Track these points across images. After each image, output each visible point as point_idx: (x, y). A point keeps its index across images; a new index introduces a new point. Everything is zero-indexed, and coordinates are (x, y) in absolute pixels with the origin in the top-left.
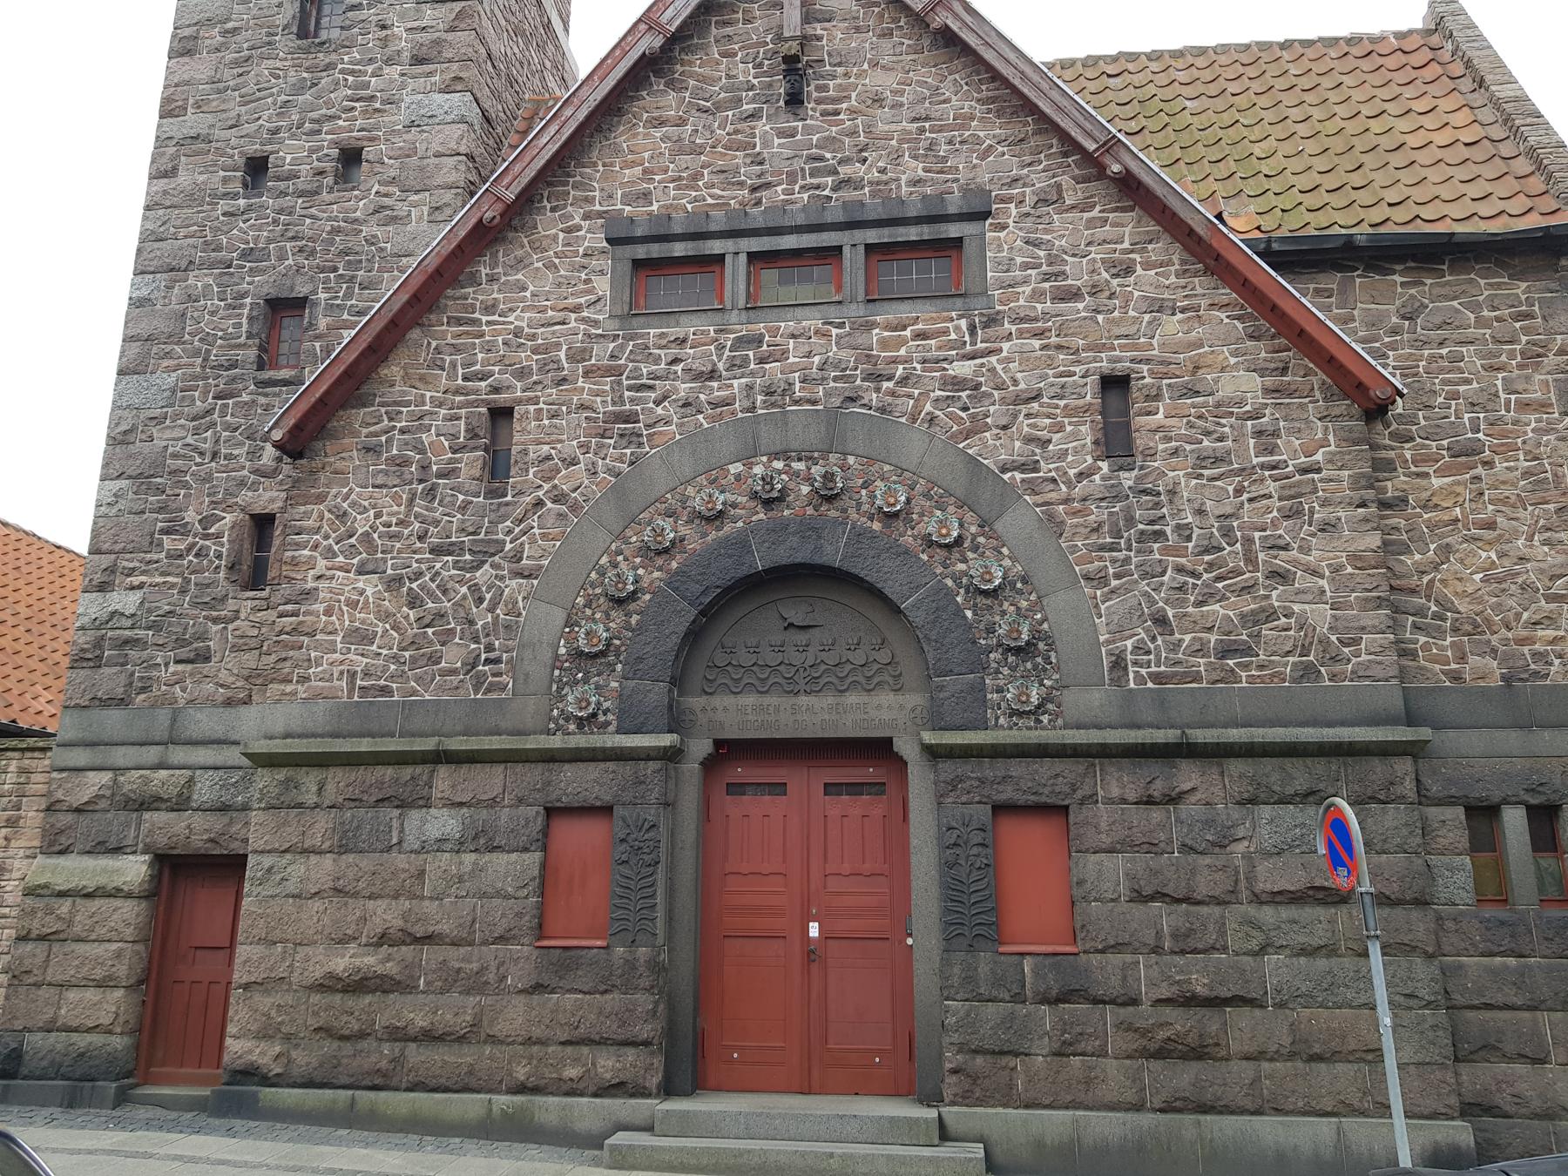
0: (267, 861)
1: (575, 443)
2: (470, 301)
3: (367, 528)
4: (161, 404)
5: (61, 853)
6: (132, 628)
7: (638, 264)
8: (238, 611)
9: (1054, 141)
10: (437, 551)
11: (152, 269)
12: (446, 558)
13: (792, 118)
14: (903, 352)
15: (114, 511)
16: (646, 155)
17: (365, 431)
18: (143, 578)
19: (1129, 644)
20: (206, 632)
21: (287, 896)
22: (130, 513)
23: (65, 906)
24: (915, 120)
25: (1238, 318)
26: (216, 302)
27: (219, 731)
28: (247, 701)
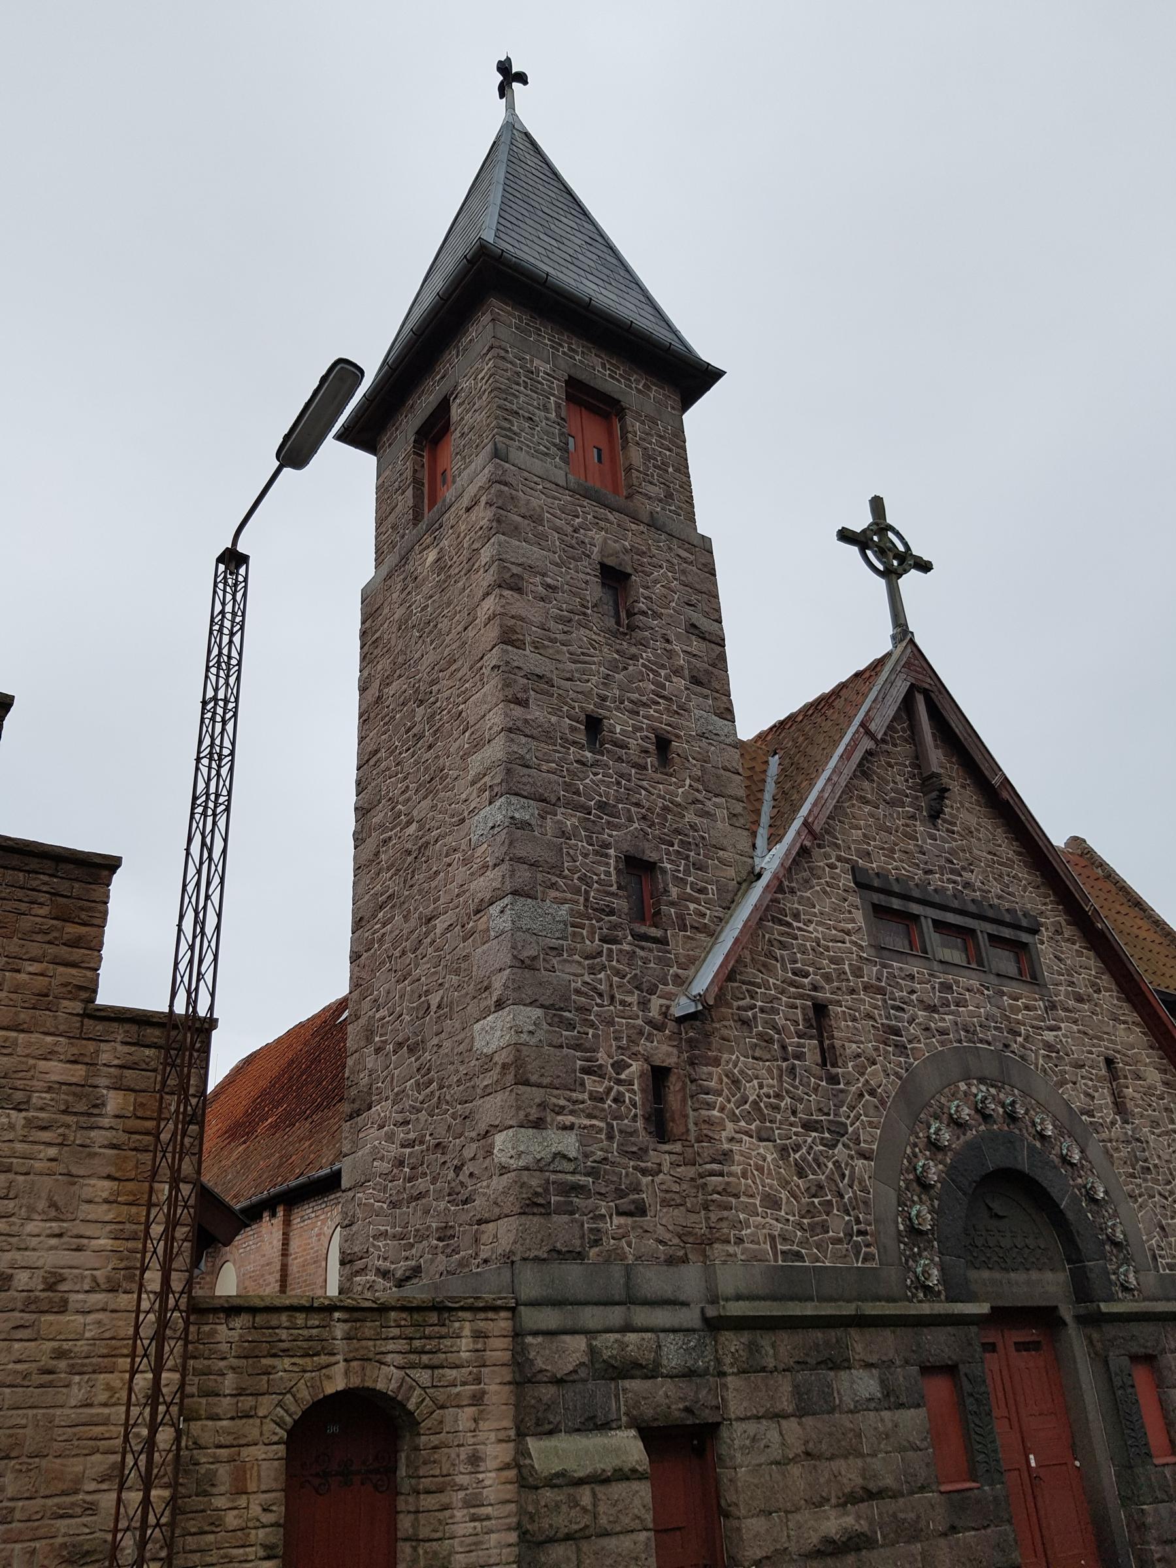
0: (751, 1427)
1: (870, 1045)
2: (781, 906)
3: (755, 1097)
4: (557, 935)
5: (550, 1433)
6: (573, 1173)
7: (874, 906)
8: (660, 1164)
9: (1051, 892)
10: (808, 1126)
11: (525, 794)
12: (814, 1134)
13: (932, 827)
14: (1020, 1017)
15: (533, 1041)
16: (862, 822)
17: (735, 1004)
18: (571, 1119)
19: (1153, 1242)
20: (639, 1183)
21: (772, 1463)
22: (550, 1045)
23: (585, 1496)
24: (990, 853)
25: (1143, 1033)
26: (585, 844)
27: (668, 1292)
28: (685, 1260)
